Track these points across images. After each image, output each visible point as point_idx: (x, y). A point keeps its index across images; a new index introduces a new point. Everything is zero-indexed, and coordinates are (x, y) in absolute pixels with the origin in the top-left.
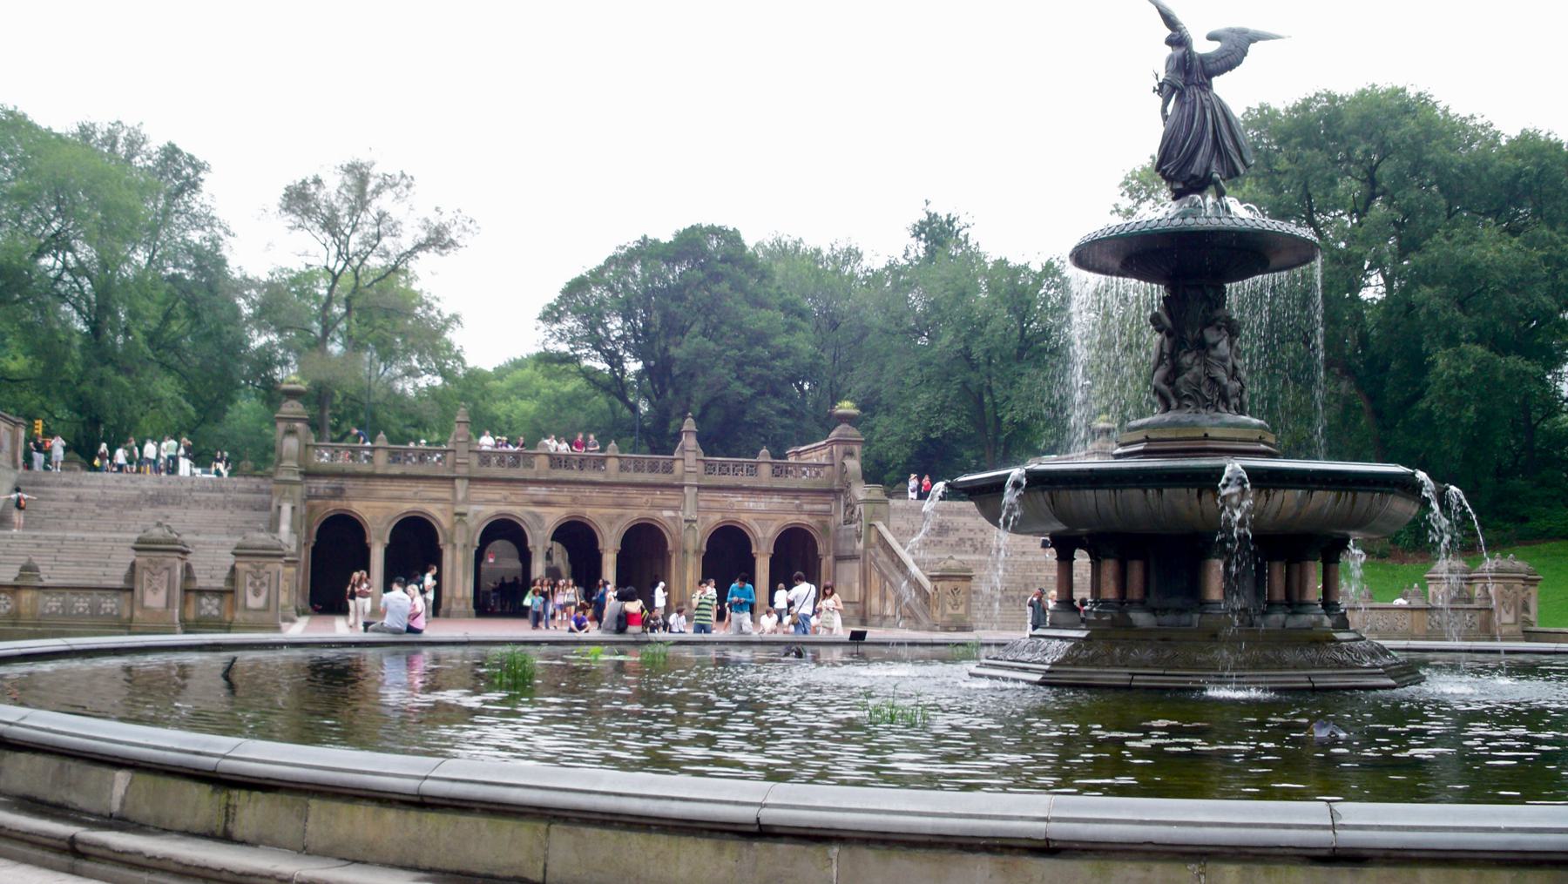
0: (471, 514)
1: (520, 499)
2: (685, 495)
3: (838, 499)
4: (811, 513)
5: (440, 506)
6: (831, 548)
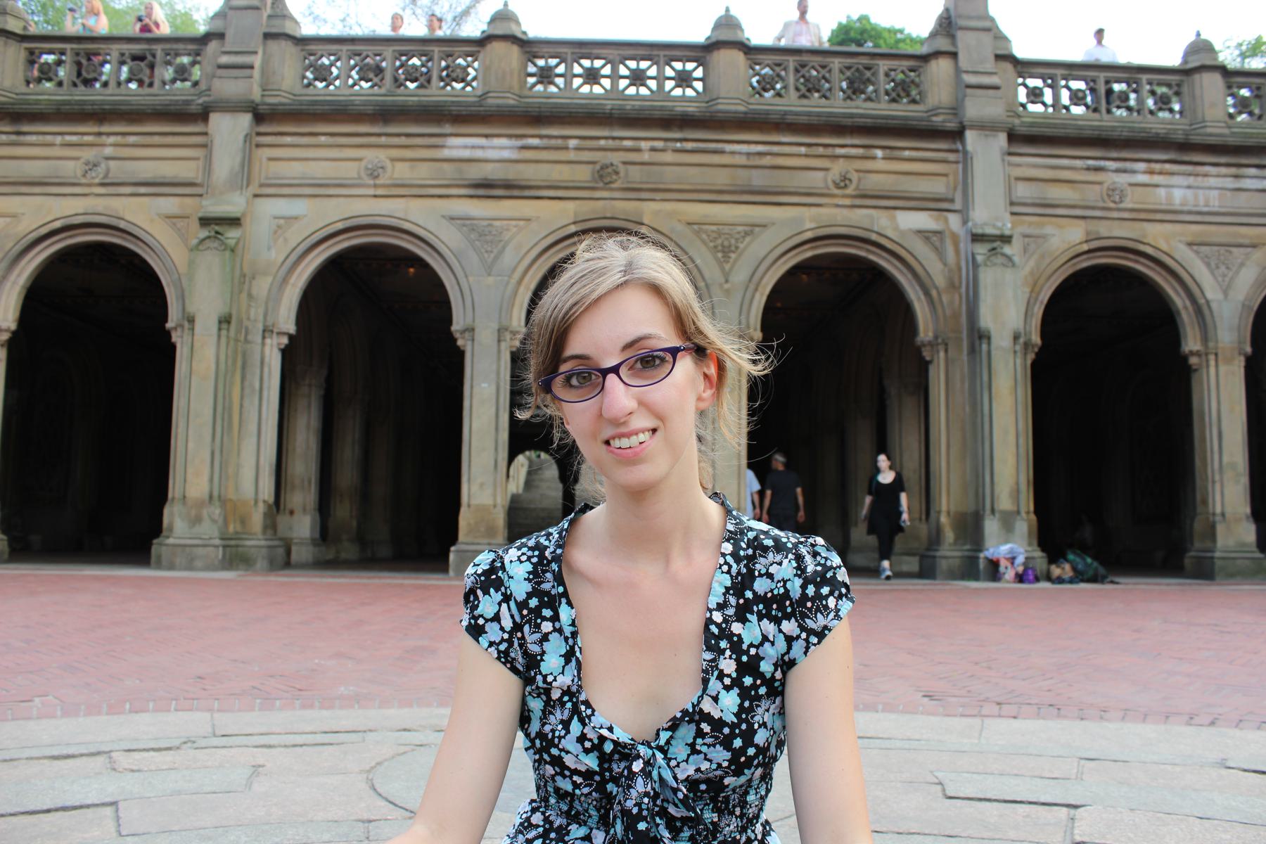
1: (423, 173)
2: (966, 159)
5: (169, 205)
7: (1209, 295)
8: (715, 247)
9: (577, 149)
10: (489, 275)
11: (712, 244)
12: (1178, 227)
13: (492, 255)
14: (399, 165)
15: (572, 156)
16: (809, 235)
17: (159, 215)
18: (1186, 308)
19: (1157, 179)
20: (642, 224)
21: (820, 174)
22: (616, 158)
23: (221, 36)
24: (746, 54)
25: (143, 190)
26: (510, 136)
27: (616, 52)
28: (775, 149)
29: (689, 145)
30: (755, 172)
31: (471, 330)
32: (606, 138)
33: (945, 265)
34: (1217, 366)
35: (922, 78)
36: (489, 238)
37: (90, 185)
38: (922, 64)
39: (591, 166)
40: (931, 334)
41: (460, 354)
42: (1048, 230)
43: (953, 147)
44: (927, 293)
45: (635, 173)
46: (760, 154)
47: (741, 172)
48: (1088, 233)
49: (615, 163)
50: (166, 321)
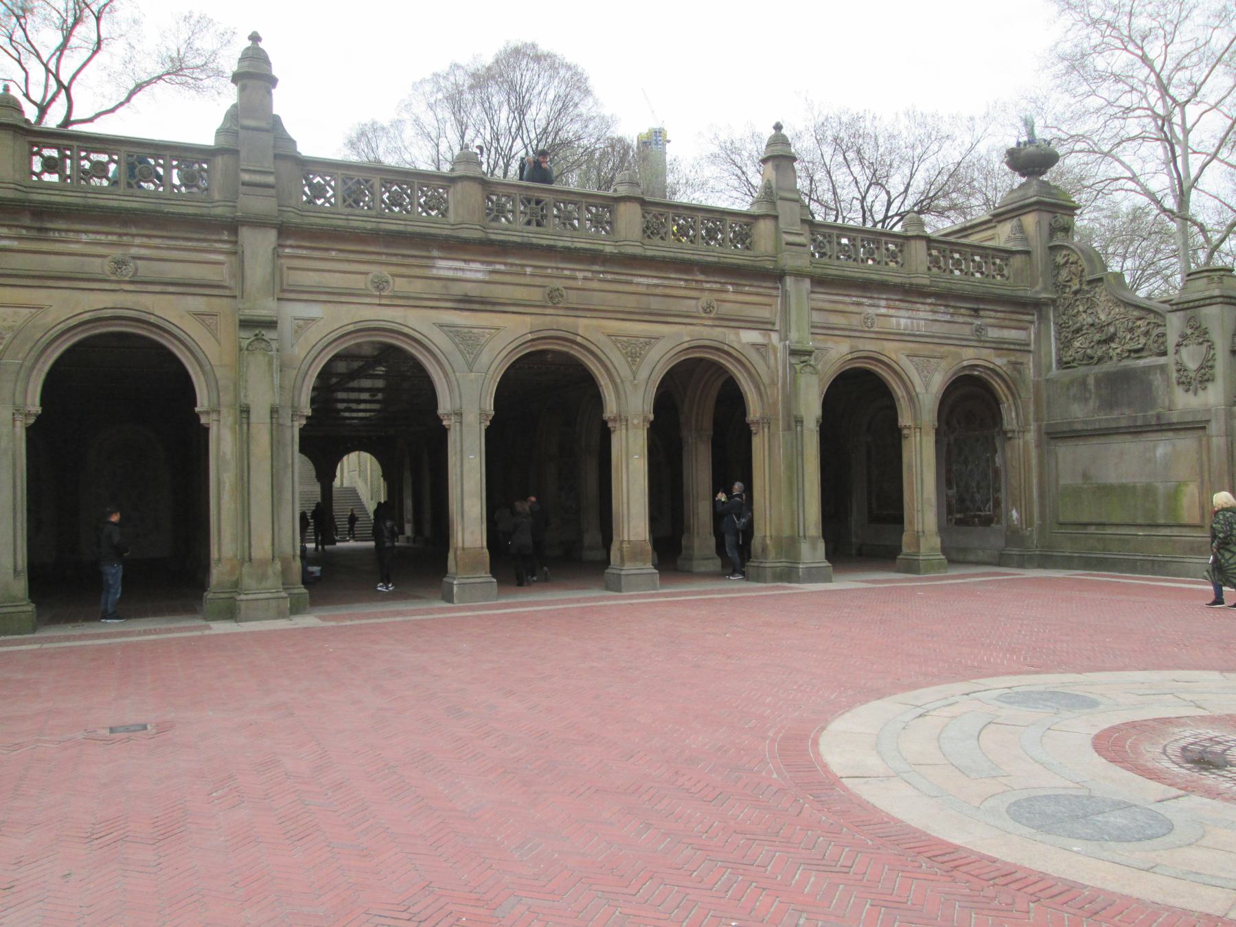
0: (286, 326)
1: (417, 287)
2: (785, 295)
3: (1043, 318)
4: (1000, 346)
6: (1031, 416)
7: (918, 390)
8: (627, 353)
9: (532, 275)
10: (471, 371)
11: (624, 351)
12: (902, 345)
13: (472, 356)
14: (398, 280)
15: (528, 280)
16: (686, 345)
17: (188, 312)
18: (903, 397)
19: (892, 312)
20: (578, 335)
21: (693, 302)
22: (558, 284)
23: (234, 152)
24: (641, 205)
25: (171, 289)
26: (482, 263)
27: (551, 197)
28: (666, 282)
29: (609, 277)
30: (652, 299)
31: (459, 414)
32: (552, 268)
33: (769, 368)
34: (921, 436)
35: (753, 231)
36: (470, 342)
37: (118, 282)
38: (754, 221)
39: (542, 289)
40: (758, 415)
41: (444, 432)
42: (830, 345)
43: (776, 285)
44: (757, 387)
45: (572, 296)
46: (656, 286)
47: (644, 299)
48: (852, 347)
49: (560, 288)
50: (195, 405)
